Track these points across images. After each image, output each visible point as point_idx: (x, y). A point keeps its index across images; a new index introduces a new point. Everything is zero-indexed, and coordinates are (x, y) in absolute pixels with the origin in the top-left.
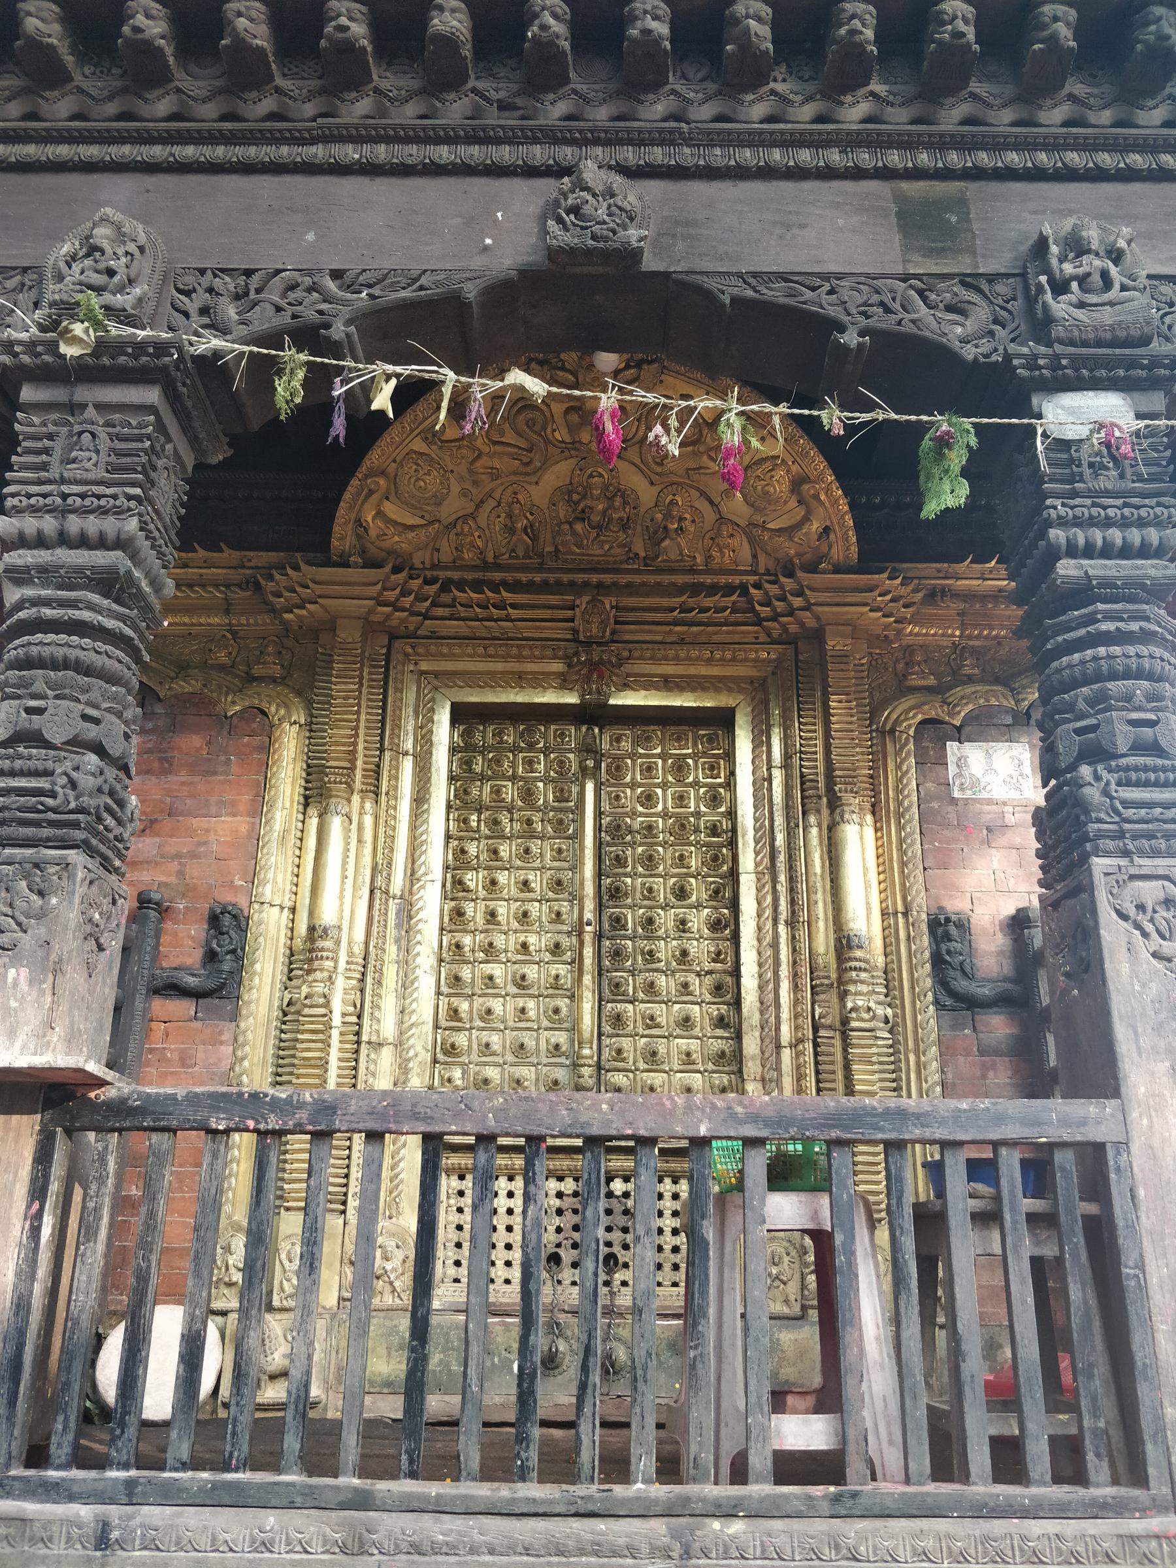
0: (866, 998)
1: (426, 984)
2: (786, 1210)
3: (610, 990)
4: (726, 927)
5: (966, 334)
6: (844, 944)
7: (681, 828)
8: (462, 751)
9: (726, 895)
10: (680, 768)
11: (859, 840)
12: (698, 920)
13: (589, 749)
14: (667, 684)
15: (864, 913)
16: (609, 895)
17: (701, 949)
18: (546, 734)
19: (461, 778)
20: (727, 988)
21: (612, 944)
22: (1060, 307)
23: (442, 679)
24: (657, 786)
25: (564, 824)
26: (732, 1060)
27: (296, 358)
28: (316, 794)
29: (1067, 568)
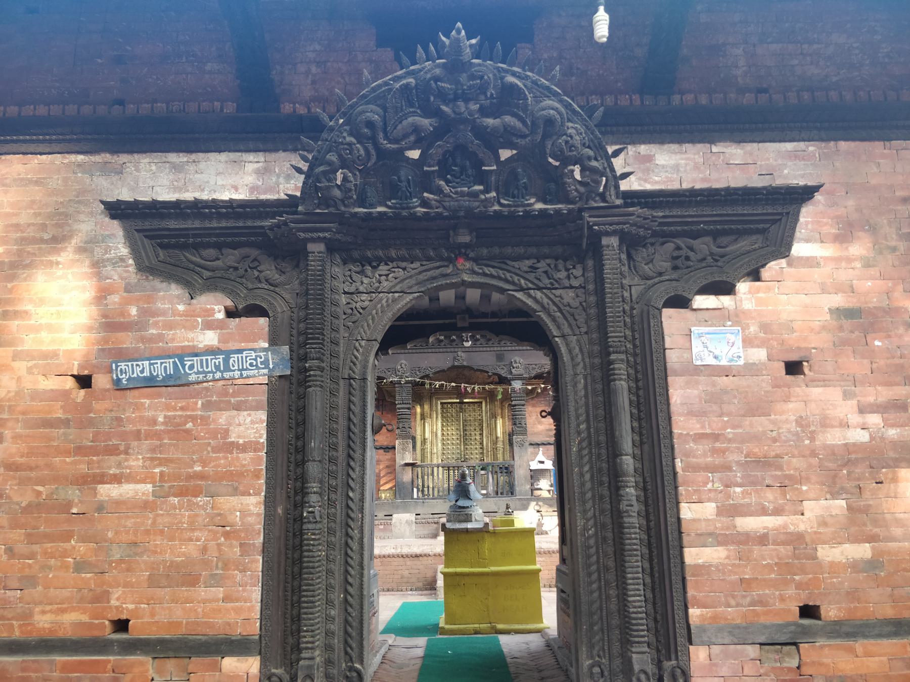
0: (500, 445)
1: (440, 445)
2: (483, 472)
3: (465, 444)
4: (481, 434)
5: (503, 373)
6: (497, 438)
7: (475, 420)
8: (442, 408)
9: (482, 430)
10: (474, 411)
11: (500, 422)
12: (478, 433)
13: (461, 408)
14: (472, 398)
15: (499, 434)
16: (465, 430)
17: (478, 437)
18: (454, 405)
19: (442, 412)
20: (482, 443)
21: (465, 438)
22: (513, 371)
23: (439, 399)
24: (471, 415)
25: (458, 420)
26: (482, 453)
27: (427, 382)
28: (423, 417)
29: (513, 403)
